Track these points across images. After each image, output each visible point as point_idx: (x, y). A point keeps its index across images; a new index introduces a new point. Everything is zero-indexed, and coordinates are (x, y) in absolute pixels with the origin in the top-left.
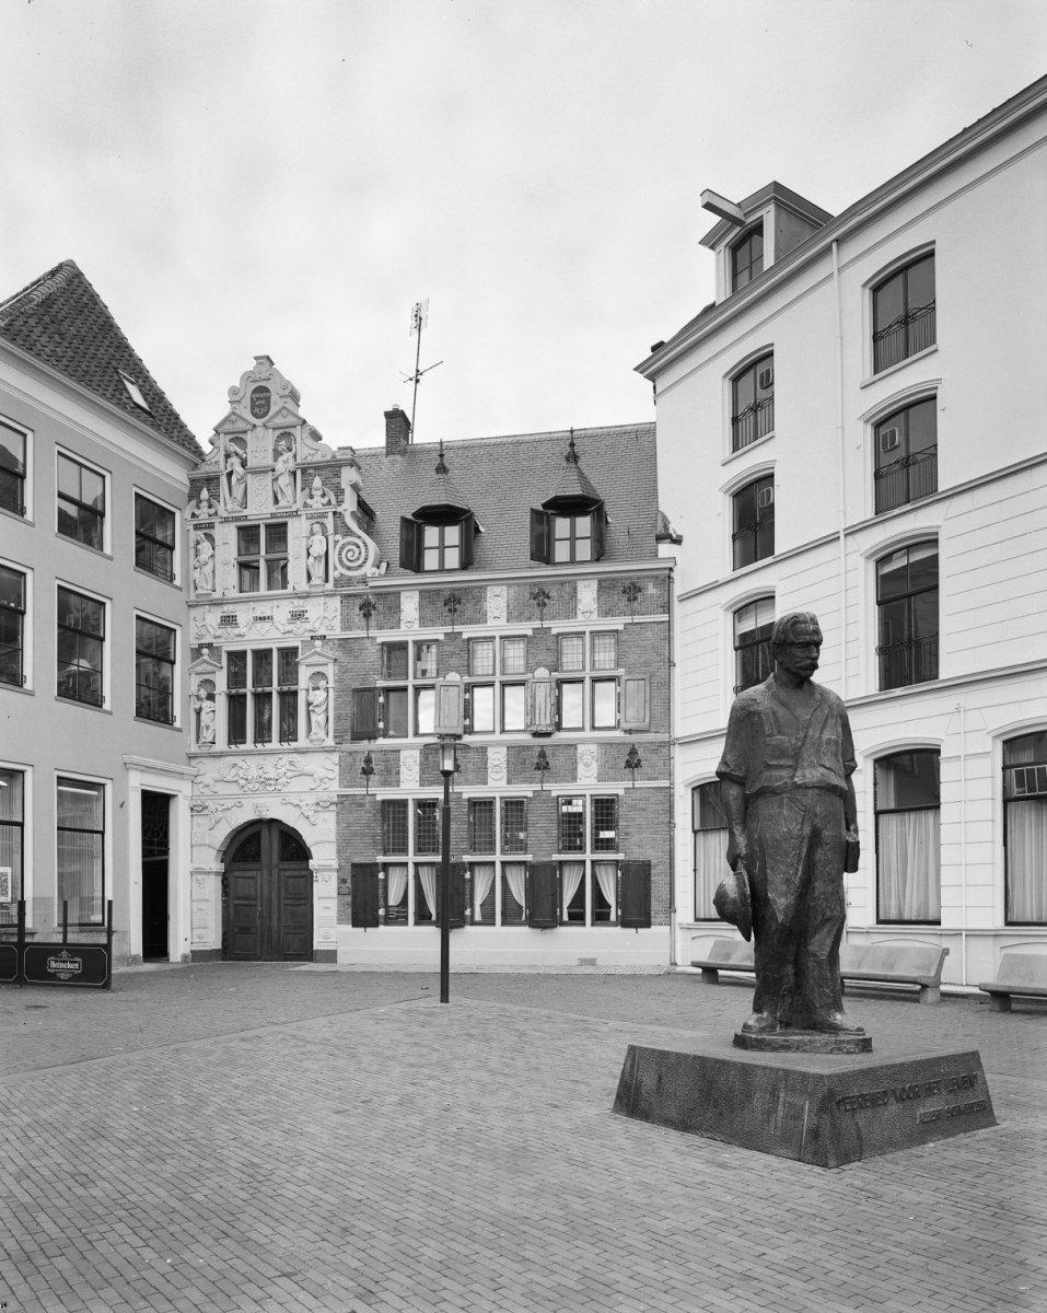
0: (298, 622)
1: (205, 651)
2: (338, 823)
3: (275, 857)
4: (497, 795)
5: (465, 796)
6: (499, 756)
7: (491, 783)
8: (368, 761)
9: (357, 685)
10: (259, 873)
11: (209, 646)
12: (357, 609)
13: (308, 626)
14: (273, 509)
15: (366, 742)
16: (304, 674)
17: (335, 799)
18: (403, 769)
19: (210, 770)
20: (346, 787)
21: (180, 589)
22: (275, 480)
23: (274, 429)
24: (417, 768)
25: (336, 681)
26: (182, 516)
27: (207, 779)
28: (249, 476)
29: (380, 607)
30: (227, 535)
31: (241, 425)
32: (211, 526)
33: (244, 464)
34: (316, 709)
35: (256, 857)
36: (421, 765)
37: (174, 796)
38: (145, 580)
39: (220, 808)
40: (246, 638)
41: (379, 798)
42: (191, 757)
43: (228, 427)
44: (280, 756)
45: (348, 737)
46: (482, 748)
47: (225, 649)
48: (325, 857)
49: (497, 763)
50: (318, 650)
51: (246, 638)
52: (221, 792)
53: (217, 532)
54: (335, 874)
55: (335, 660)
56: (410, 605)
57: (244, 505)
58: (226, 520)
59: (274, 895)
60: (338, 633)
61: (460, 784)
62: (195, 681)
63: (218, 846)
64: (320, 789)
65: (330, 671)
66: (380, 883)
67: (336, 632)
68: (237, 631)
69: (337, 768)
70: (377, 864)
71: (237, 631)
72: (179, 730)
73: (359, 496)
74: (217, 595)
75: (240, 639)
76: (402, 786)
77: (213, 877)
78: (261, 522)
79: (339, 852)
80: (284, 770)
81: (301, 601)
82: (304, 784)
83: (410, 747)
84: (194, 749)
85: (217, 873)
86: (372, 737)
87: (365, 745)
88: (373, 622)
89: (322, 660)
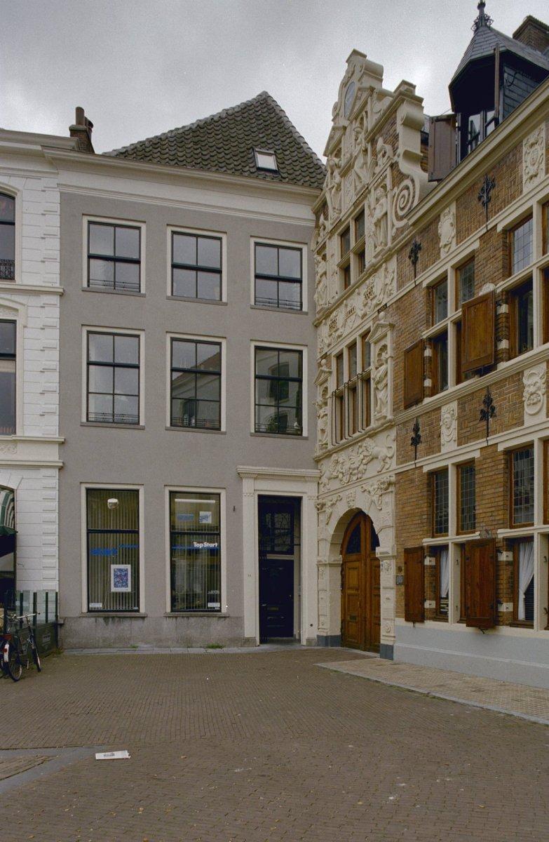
0: (369, 301)
1: (324, 361)
2: (396, 505)
4: (535, 438)
5: (501, 448)
6: (536, 379)
7: (528, 421)
8: (416, 429)
9: (409, 345)
11: (325, 356)
12: (407, 259)
13: (375, 302)
15: (414, 408)
16: (374, 350)
17: (393, 479)
18: (443, 430)
19: (327, 467)
20: (402, 463)
21: (306, 314)
24: (455, 424)
25: (394, 349)
26: (309, 249)
27: (324, 480)
29: (424, 245)
30: (334, 246)
32: (324, 247)
34: (379, 386)
36: (459, 418)
40: (343, 336)
41: (425, 470)
42: (318, 461)
44: (359, 444)
45: (402, 408)
46: (518, 373)
47: (334, 354)
48: (387, 545)
49: (532, 389)
50: (382, 322)
51: (343, 336)
52: (332, 489)
53: (328, 251)
54: (393, 564)
55: (392, 326)
56: (446, 228)
58: (332, 233)
59: (368, 584)
60: (397, 294)
61: (495, 432)
62: (320, 390)
63: (330, 539)
64: (384, 471)
65: (388, 341)
66: (427, 572)
67: (392, 296)
68: (338, 333)
69: (394, 446)
70: (422, 548)
71: (338, 333)
72: (306, 438)
73: (422, 132)
75: (341, 338)
76: (444, 450)
77: (328, 568)
78: (350, 219)
79: (397, 537)
80: (362, 456)
82: (373, 469)
83: (447, 401)
84: (318, 453)
85: (331, 565)
86: (418, 401)
87: (415, 410)
88: (419, 266)
89: (384, 329)
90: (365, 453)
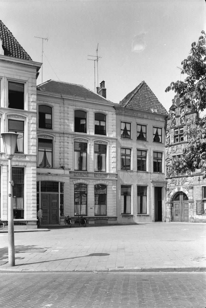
3: (182, 199)
10: (174, 203)
14: (180, 124)
22: (181, 118)
23: (181, 107)
28: (176, 118)
31: (175, 107)
33: (175, 115)
35: (179, 199)
37: (162, 187)
38: (156, 144)
39: (171, 189)
43: (172, 108)
57: (175, 124)
74: (170, 144)
81: (186, 144)
90: (185, 180)
